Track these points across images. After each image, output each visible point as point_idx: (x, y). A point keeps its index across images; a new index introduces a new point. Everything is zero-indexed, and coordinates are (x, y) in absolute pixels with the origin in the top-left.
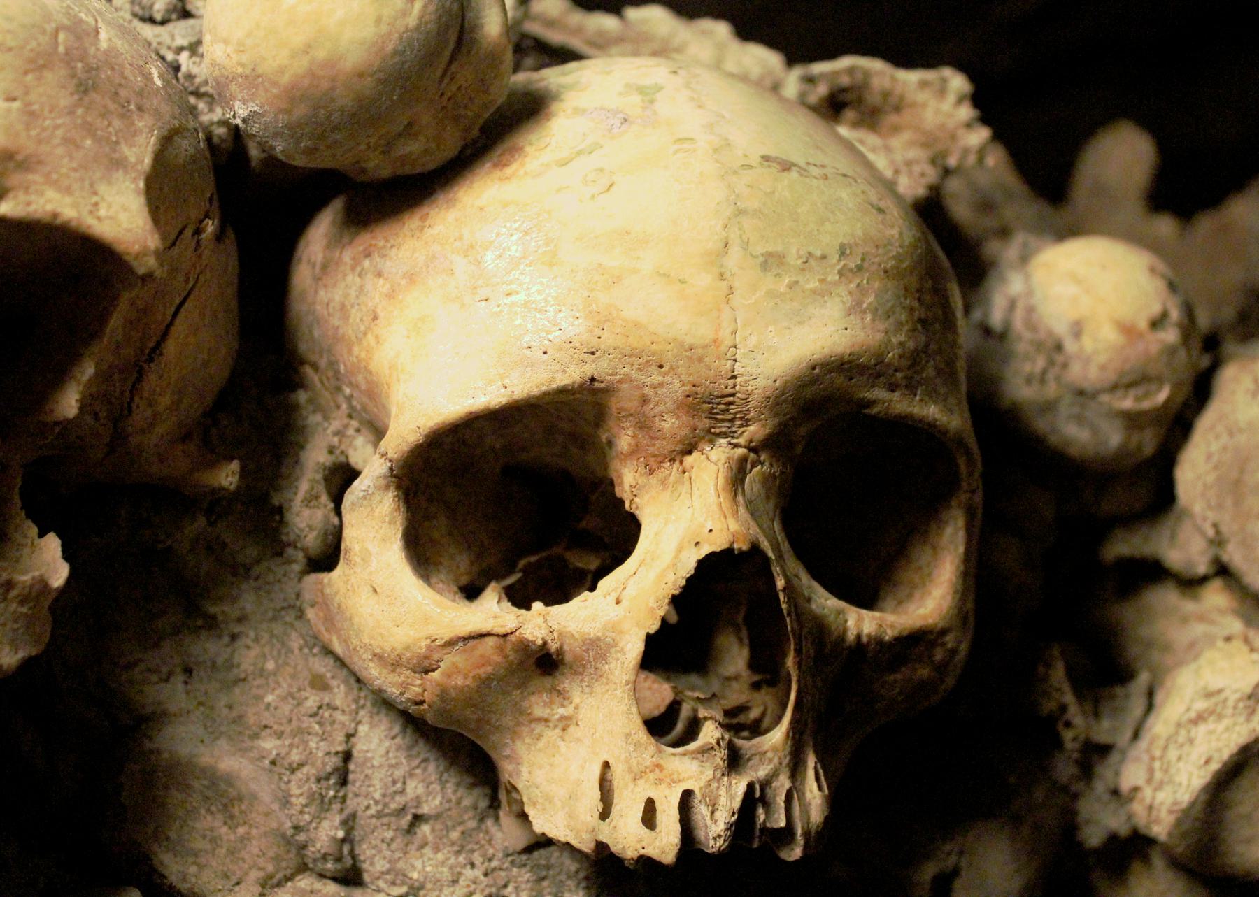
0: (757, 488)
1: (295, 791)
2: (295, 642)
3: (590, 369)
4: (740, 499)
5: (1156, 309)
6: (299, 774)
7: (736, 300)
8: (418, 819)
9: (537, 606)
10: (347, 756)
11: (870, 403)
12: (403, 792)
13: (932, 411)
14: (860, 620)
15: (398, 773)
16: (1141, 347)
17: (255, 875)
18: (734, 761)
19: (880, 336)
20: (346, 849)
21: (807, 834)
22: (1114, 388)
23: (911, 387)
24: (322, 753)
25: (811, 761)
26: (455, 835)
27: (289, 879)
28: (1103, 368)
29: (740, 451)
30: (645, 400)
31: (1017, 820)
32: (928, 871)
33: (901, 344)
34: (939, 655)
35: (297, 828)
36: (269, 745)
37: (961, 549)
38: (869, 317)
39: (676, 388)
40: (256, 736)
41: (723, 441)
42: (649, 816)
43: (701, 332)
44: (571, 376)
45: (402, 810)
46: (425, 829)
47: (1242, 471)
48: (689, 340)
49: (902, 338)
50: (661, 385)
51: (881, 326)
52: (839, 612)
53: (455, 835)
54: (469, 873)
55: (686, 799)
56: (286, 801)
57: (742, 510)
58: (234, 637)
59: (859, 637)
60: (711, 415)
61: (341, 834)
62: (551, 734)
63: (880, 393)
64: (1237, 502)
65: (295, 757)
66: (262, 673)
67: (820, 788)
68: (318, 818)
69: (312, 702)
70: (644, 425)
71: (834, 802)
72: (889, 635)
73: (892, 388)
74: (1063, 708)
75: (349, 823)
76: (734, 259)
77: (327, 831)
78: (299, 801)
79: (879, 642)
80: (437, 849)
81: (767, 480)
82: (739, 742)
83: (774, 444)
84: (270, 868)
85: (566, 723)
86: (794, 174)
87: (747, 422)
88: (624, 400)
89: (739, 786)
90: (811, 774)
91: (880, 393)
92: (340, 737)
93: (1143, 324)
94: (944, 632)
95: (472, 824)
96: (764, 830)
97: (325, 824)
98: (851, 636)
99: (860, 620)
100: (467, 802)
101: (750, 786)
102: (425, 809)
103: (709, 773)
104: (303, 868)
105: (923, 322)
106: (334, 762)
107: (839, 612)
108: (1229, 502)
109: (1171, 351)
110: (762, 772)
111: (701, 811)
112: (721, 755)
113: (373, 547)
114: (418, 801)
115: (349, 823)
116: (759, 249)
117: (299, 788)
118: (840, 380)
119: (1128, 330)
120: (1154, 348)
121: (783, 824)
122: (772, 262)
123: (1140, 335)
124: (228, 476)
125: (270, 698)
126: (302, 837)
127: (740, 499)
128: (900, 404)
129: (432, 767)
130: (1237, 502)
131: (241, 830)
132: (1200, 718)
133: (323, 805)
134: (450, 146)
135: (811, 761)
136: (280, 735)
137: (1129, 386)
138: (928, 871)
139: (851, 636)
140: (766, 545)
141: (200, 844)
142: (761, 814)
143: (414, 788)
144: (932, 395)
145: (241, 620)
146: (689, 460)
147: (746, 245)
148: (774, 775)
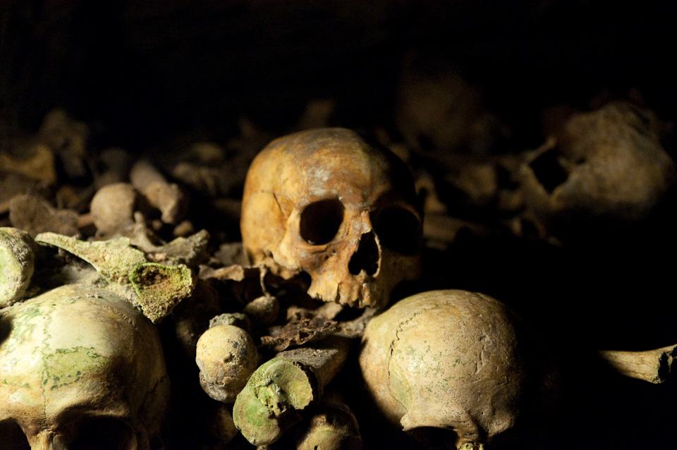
0: (57, 441)
3: (10, 415)
4: (51, 445)
5: (227, 355)
7: (45, 393)
11: (89, 414)
13: (111, 412)
19: (89, 396)
23: (102, 408)
30: (24, 422)
33: (98, 396)
38: (86, 391)
41: (45, 430)
48: (33, 406)
49: (99, 394)
50: (25, 418)
51: (90, 393)
60: (40, 424)
63: (91, 412)
70: (26, 427)
73: (95, 409)
81: (60, 438)
87: (51, 425)
88: (20, 422)
91: (91, 412)
93: (222, 361)
109: (235, 367)
118: (75, 411)
119: (217, 364)
123: (222, 365)
127: (51, 445)
128: (98, 413)
144: (111, 407)
146: (38, 435)
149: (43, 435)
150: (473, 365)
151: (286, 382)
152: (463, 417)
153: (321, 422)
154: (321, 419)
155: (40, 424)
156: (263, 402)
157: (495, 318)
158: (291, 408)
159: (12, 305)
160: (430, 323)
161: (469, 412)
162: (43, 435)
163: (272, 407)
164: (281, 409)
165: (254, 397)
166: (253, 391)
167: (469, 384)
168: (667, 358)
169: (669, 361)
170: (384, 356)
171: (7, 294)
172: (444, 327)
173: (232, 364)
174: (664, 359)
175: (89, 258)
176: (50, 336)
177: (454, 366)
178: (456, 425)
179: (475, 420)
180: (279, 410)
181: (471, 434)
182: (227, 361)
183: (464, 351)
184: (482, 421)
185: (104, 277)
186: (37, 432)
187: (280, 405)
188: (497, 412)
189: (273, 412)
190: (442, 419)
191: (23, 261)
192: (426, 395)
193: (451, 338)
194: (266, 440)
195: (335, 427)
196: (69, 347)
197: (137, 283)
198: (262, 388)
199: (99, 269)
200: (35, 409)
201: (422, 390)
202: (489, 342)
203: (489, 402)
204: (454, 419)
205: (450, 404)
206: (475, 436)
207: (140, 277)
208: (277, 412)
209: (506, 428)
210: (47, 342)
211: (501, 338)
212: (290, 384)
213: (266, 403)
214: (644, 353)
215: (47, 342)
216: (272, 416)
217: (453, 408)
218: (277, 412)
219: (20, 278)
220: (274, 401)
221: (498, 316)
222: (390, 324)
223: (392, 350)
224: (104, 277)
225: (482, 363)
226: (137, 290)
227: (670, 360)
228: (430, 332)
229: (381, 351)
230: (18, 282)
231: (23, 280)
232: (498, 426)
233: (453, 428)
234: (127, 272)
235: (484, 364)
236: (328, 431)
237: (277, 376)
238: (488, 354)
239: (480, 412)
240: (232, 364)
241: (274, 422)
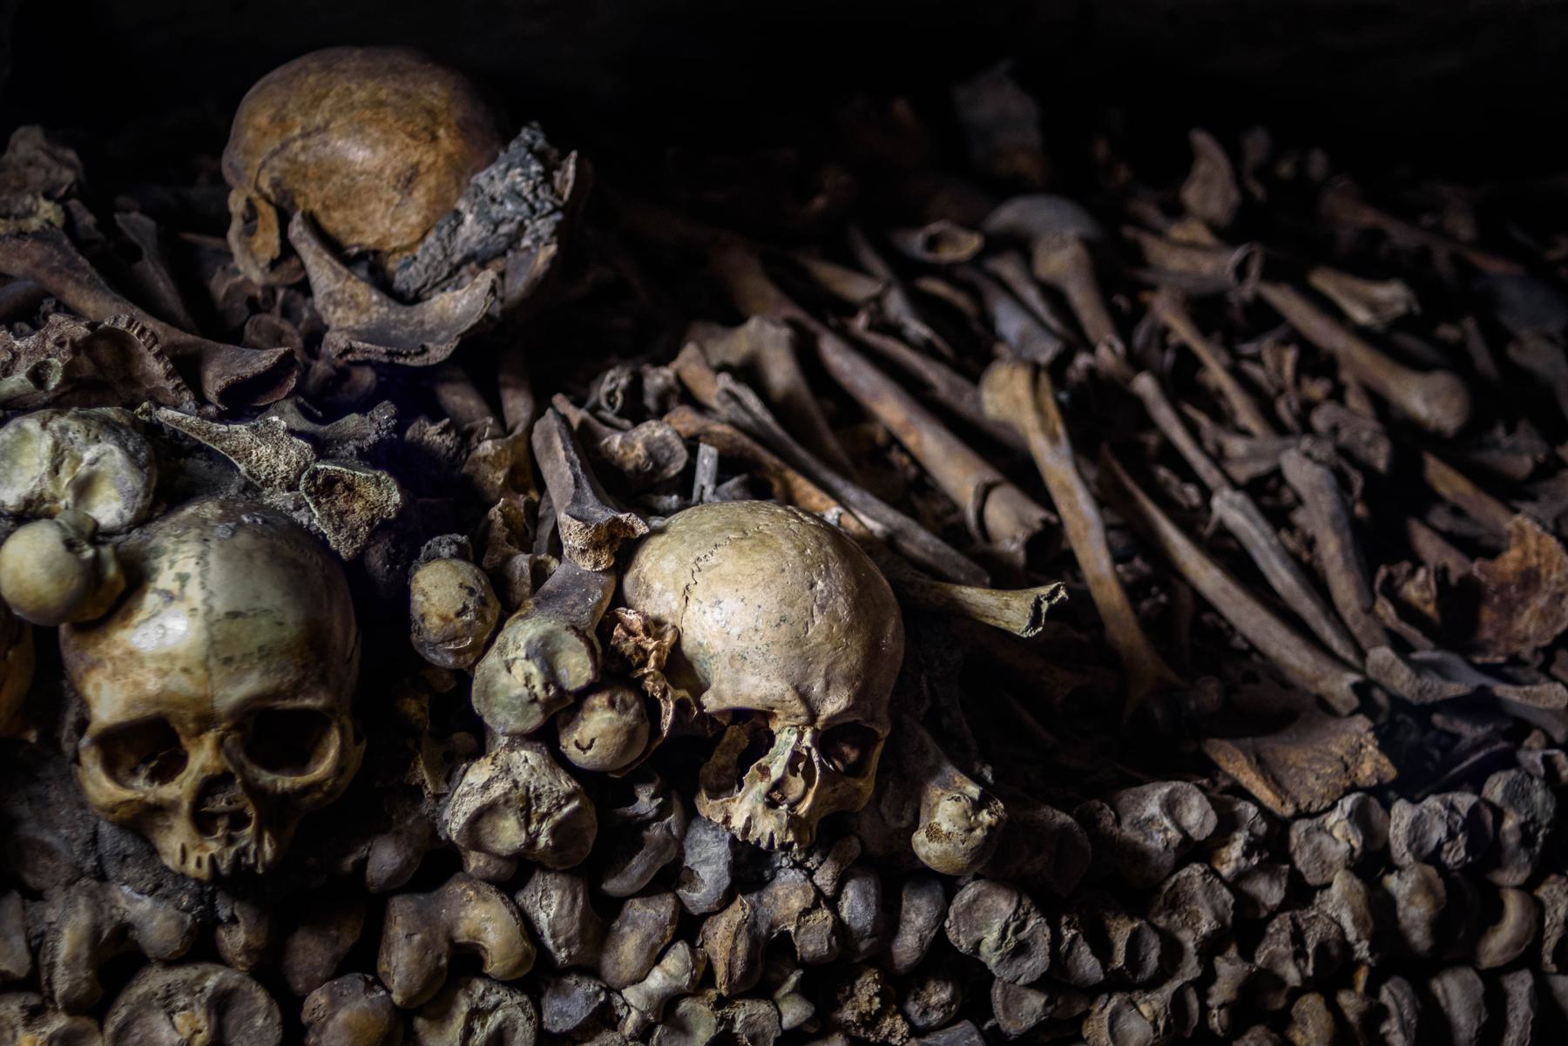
1: (75, 849)
2: (71, 790)
4: (222, 751)
5: (460, 606)
6: (76, 843)
8: (125, 857)
9: (156, 783)
10: (96, 833)
12: (118, 846)
13: (308, 702)
14: (283, 783)
15: (116, 839)
16: (451, 626)
17: (63, 880)
18: (230, 841)
20: (98, 869)
21: (264, 865)
22: (443, 642)
23: (294, 696)
24: (85, 833)
25: (267, 836)
26: (140, 862)
27: (78, 880)
28: (436, 635)
29: (220, 733)
31: (398, 833)
32: (351, 859)
34: (325, 788)
35: (78, 863)
36: (64, 831)
37: (338, 743)
39: (191, 714)
40: (58, 828)
42: (199, 863)
43: (201, 692)
44: (152, 711)
45: (118, 854)
46: (129, 859)
47: (487, 687)
49: (289, 677)
52: (274, 782)
53: (140, 862)
54: (147, 876)
55: (212, 859)
56: (72, 852)
57: (223, 756)
58: (48, 786)
59: (283, 789)
61: (95, 864)
62: (166, 831)
64: (486, 700)
65: (74, 836)
66: (58, 802)
67: (271, 846)
68: (85, 859)
69: (79, 814)
70: (183, 726)
71: (277, 853)
72: (297, 787)
73: (285, 699)
74: (424, 781)
75: (100, 859)
76: (212, 662)
77: (90, 863)
78: (77, 853)
79: (292, 789)
80: (134, 867)
82: (234, 833)
83: (238, 726)
84: (70, 876)
85: (170, 828)
86: (239, 620)
87: (221, 722)
89: (232, 850)
90: (266, 842)
92: (91, 827)
93: (452, 615)
94: (326, 780)
95: (147, 857)
96: (246, 865)
97: (88, 861)
98: (279, 789)
99: (283, 783)
100: (145, 848)
101: (237, 851)
102: (129, 852)
103: (220, 847)
104: (82, 875)
105: (303, 666)
106: (90, 836)
107: (274, 782)
108: (482, 699)
109: (470, 624)
110: (244, 843)
111: (219, 861)
112: (223, 841)
113: (90, 765)
114: (125, 850)
115: (100, 859)
116: (223, 655)
117: (77, 848)
120: (459, 625)
121: (252, 861)
122: (228, 661)
123: (451, 620)
124: (32, 737)
125: (62, 813)
126: (80, 866)
128: (289, 704)
129: (130, 836)
130: (486, 700)
131: (56, 864)
132: (464, 795)
133: (86, 853)
134: (102, 611)
135: (267, 836)
136: (67, 828)
137: (450, 641)
138: (351, 859)
139: (279, 789)
140: (231, 768)
141: (40, 870)
142: (243, 860)
143: (123, 844)
144: (308, 694)
145: (50, 778)
146: (202, 736)
147: (216, 655)
148: (248, 845)
149: (209, 739)
150: (801, 625)
151: (554, 653)
152: (789, 696)
153: (600, 707)
154: (599, 700)
155: (206, 721)
156: (521, 680)
157: (826, 554)
158: (561, 690)
159: (129, 531)
160: (742, 562)
161: (797, 688)
162: (209, 739)
163: (533, 687)
164: (548, 691)
165: (504, 672)
166: (503, 664)
167: (798, 651)
168: (1041, 603)
169: (1042, 606)
170: (675, 605)
171: (121, 516)
172: (762, 569)
173: (467, 618)
174: (1038, 603)
175: (222, 449)
176: (211, 593)
177: (778, 625)
178: (779, 705)
179: (804, 697)
180: (544, 692)
181: (797, 716)
182: (459, 614)
183: (791, 605)
184: (813, 698)
185: (251, 479)
186: (200, 732)
187: (546, 687)
188: (832, 687)
189: (535, 694)
190: (760, 697)
191: (145, 466)
192: (738, 665)
193: (772, 586)
194: (520, 730)
195: (619, 712)
196: (243, 608)
197: (309, 494)
198: (518, 663)
199: (242, 468)
200: (197, 701)
201: (732, 657)
202: (822, 591)
203: (823, 673)
204: (777, 697)
205: (771, 678)
206: (803, 719)
207: (315, 484)
208: (542, 695)
209: (842, 707)
210: (210, 602)
211: (837, 584)
212: (559, 655)
213: (524, 682)
214: (1009, 593)
215: (210, 602)
216: (534, 700)
217: (775, 683)
218: (542, 695)
219: (142, 494)
220: (538, 682)
221: (829, 549)
222: (680, 559)
223: (687, 598)
224: (251, 479)
225: (814, 622)
226: (312, 505)
227: (1045, 606)
228: (743, 575)
229: (670, 596)
230: (139, 499)
231: (146, 496)
232: (834, 704)
233: (773, 708)
234: (287, 472)
235: (817, 623)
236: (610, 718)
237: (542, 646)
238: (822, 608)
239: (810, 688)
240: (467, 618)
241: (537, 708)
